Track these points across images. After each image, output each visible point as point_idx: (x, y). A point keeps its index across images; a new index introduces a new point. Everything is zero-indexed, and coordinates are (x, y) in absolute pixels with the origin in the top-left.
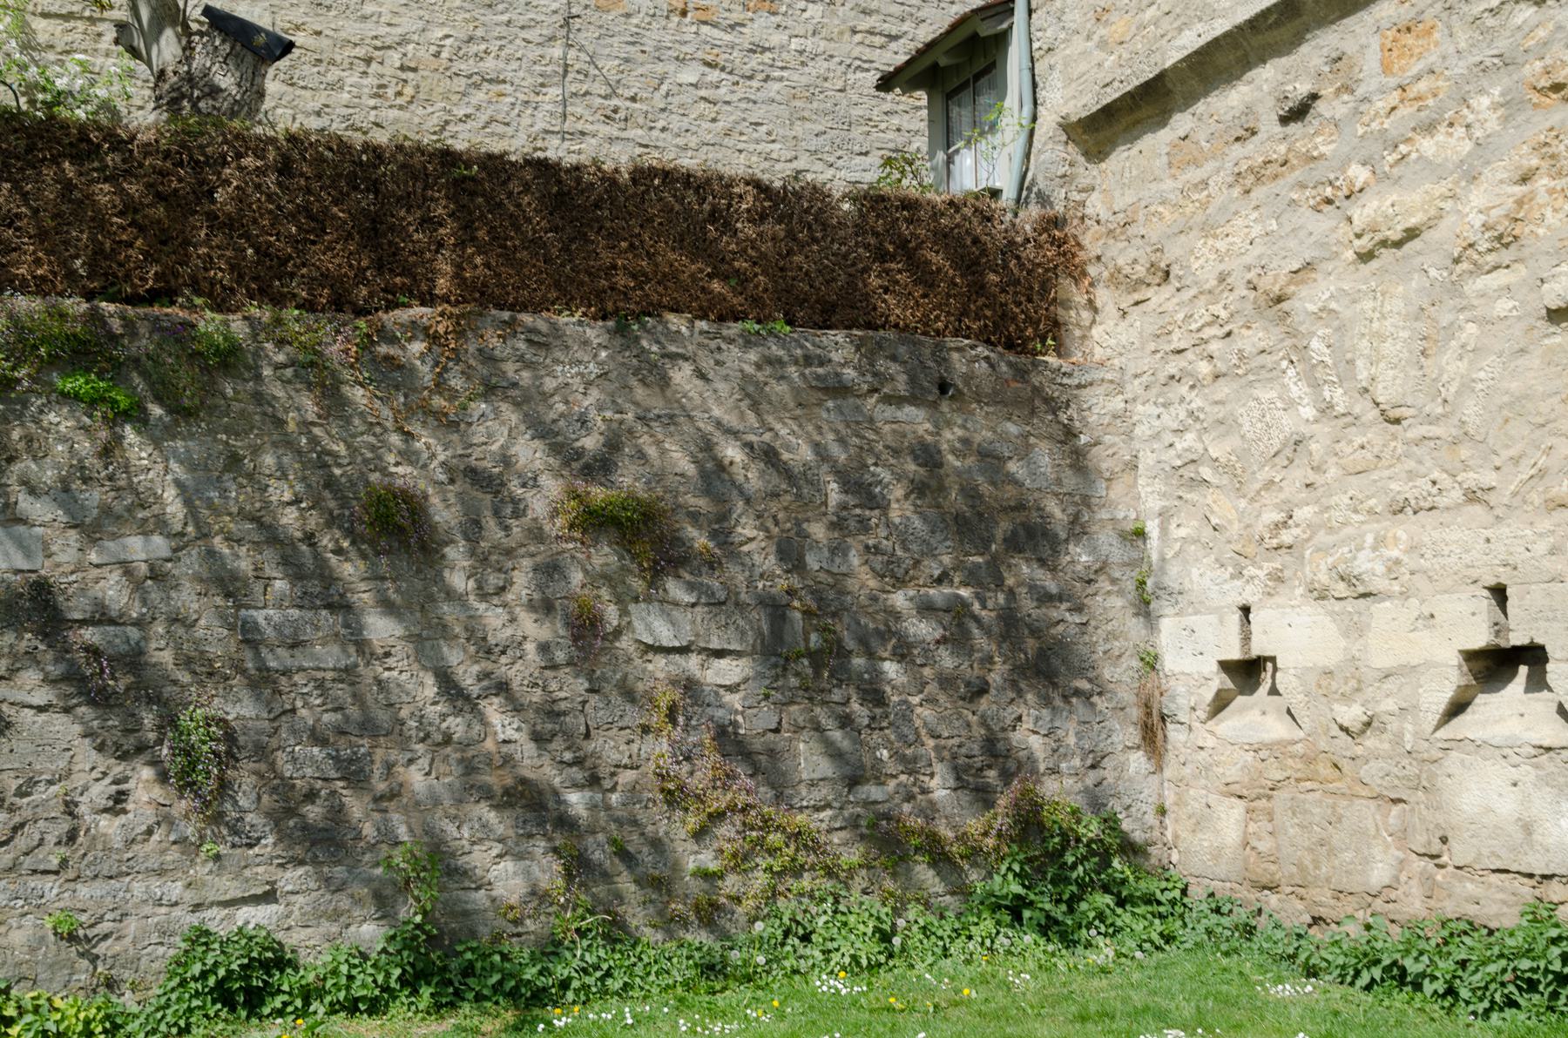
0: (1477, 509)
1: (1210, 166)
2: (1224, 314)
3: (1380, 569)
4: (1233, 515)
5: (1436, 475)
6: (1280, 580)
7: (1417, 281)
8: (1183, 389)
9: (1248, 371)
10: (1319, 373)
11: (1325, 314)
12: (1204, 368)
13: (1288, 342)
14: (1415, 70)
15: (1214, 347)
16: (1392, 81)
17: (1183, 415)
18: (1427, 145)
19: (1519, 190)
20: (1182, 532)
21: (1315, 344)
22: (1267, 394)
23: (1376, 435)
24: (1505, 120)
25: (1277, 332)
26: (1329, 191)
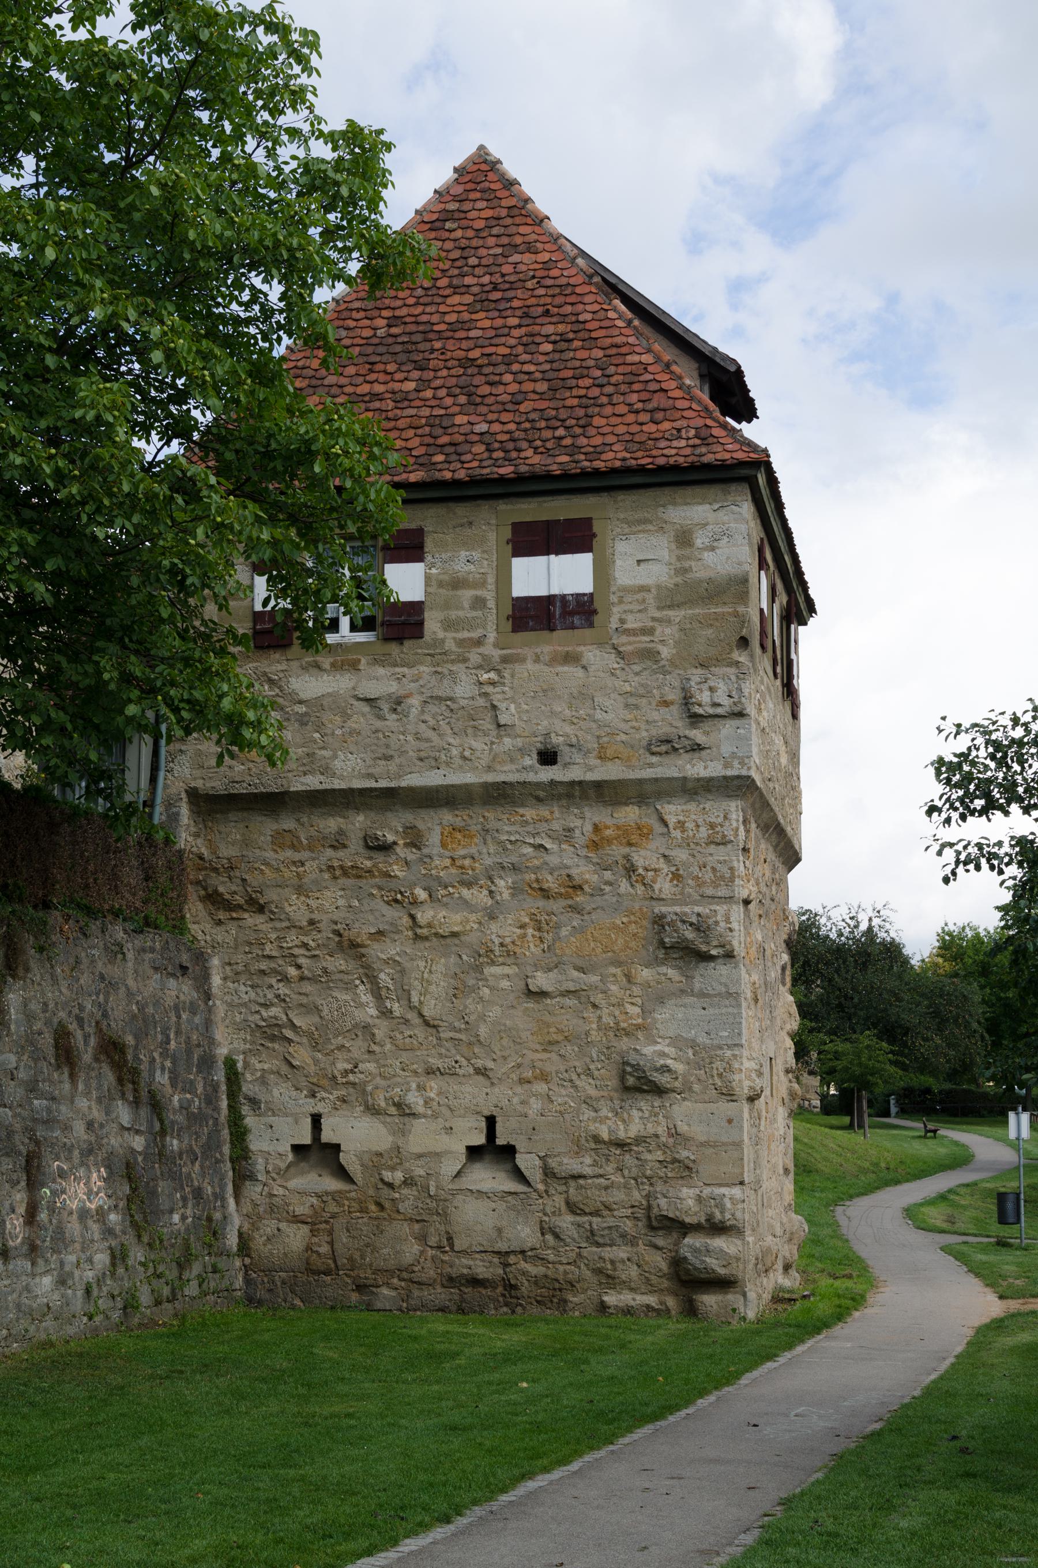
0: (480, 1078)
1: (304, 855)
2: (311, 943)
3: (421, 1102)
4: (309, 1061)
5: (458, 1058)
6: (344, 1101)
7: (453, 959)
8: (273, 981)
9: (324, 979)
10: (383, 993)
11: (390, 961)
12: (292, 972)
13: (361, 971)
14: (462, 852)
15: (302, 961)
16: (447, 853)
17: (270, 996)
18: (465, 892)
19: (518, 931)
20: (266, 1066)
21: (382, 976)
22: (344, 996)
23: (420, 1032)
24: (513, 895)
25: (352, 965)
26: (399, 896)
